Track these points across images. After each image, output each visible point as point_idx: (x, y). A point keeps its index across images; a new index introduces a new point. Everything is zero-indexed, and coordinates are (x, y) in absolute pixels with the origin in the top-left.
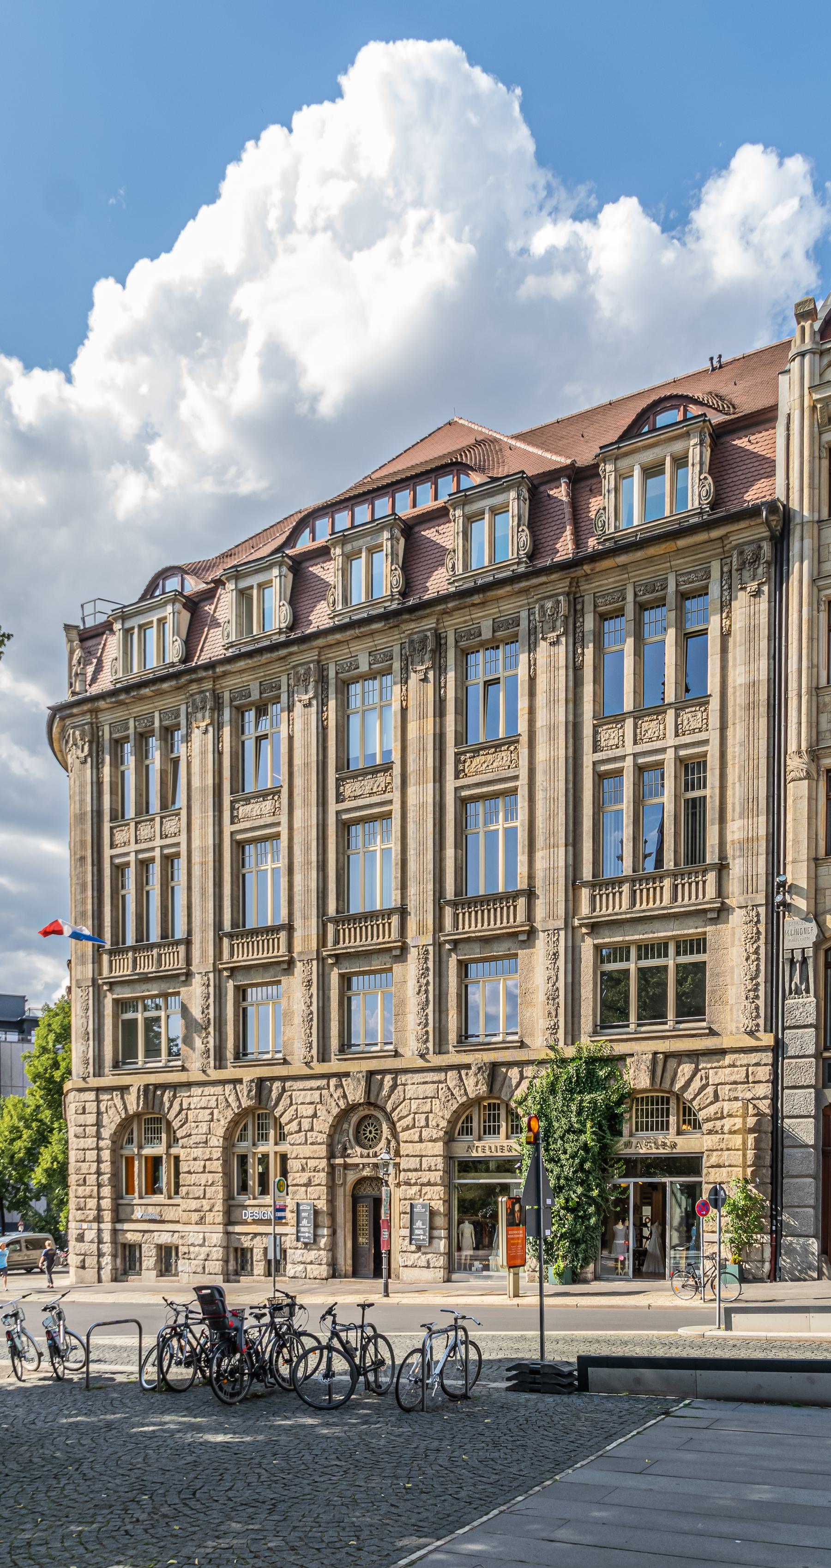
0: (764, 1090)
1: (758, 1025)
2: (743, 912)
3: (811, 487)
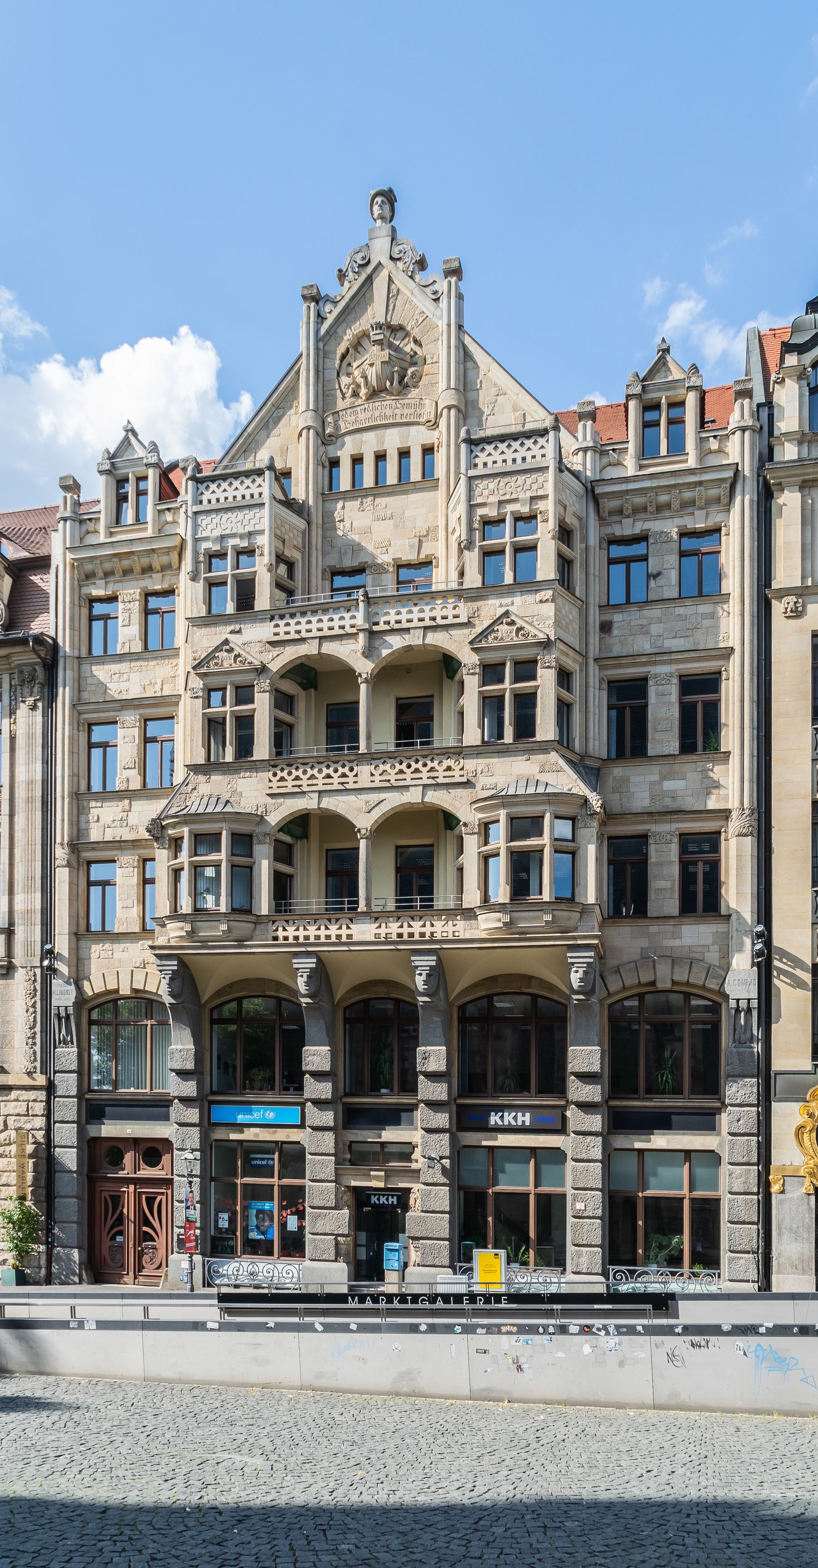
0: (40, 1122)
1: (35, 1068)
3: (72, 628)
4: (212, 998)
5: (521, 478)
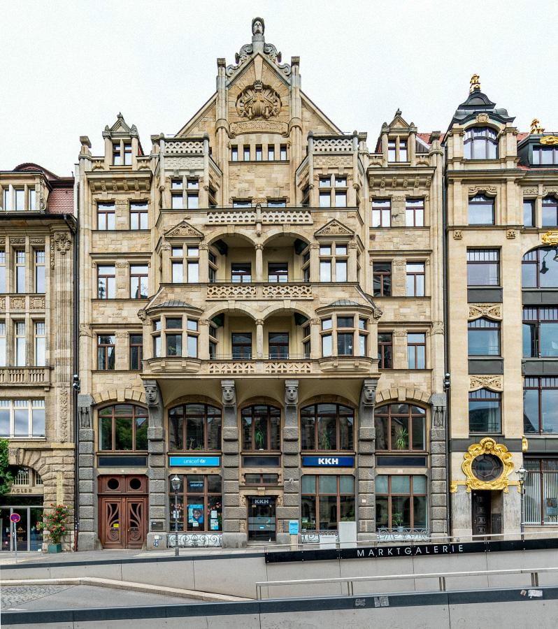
2: (61, 389)
4: (170, 404)
5: (345, 157)
